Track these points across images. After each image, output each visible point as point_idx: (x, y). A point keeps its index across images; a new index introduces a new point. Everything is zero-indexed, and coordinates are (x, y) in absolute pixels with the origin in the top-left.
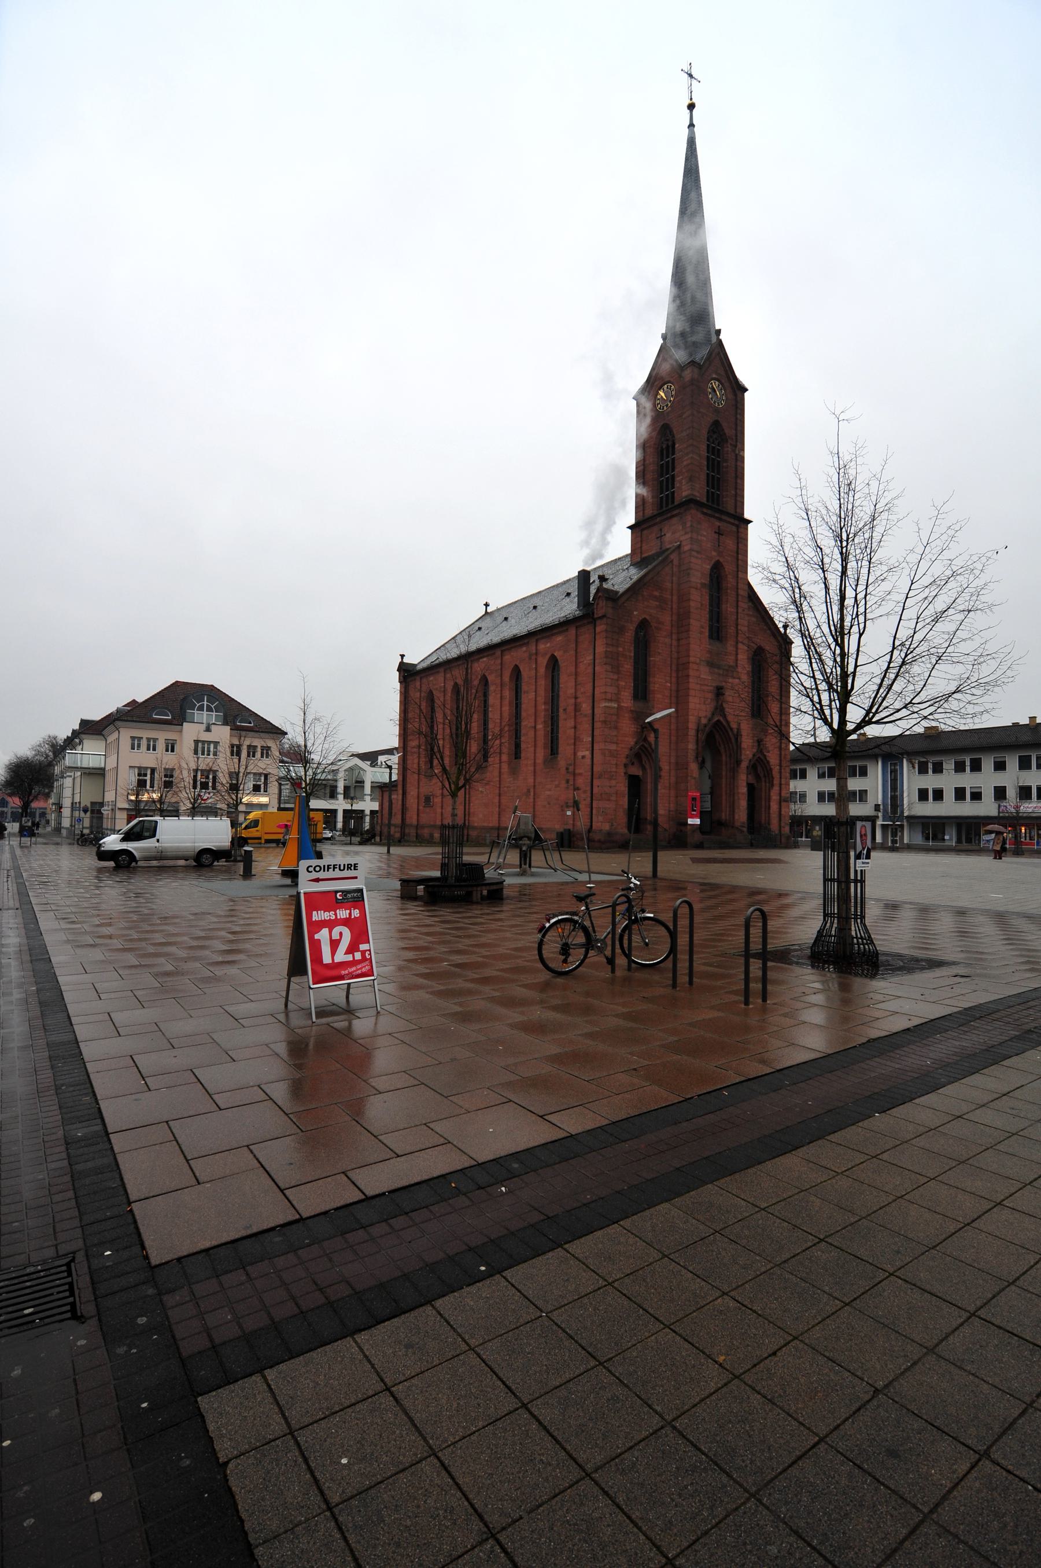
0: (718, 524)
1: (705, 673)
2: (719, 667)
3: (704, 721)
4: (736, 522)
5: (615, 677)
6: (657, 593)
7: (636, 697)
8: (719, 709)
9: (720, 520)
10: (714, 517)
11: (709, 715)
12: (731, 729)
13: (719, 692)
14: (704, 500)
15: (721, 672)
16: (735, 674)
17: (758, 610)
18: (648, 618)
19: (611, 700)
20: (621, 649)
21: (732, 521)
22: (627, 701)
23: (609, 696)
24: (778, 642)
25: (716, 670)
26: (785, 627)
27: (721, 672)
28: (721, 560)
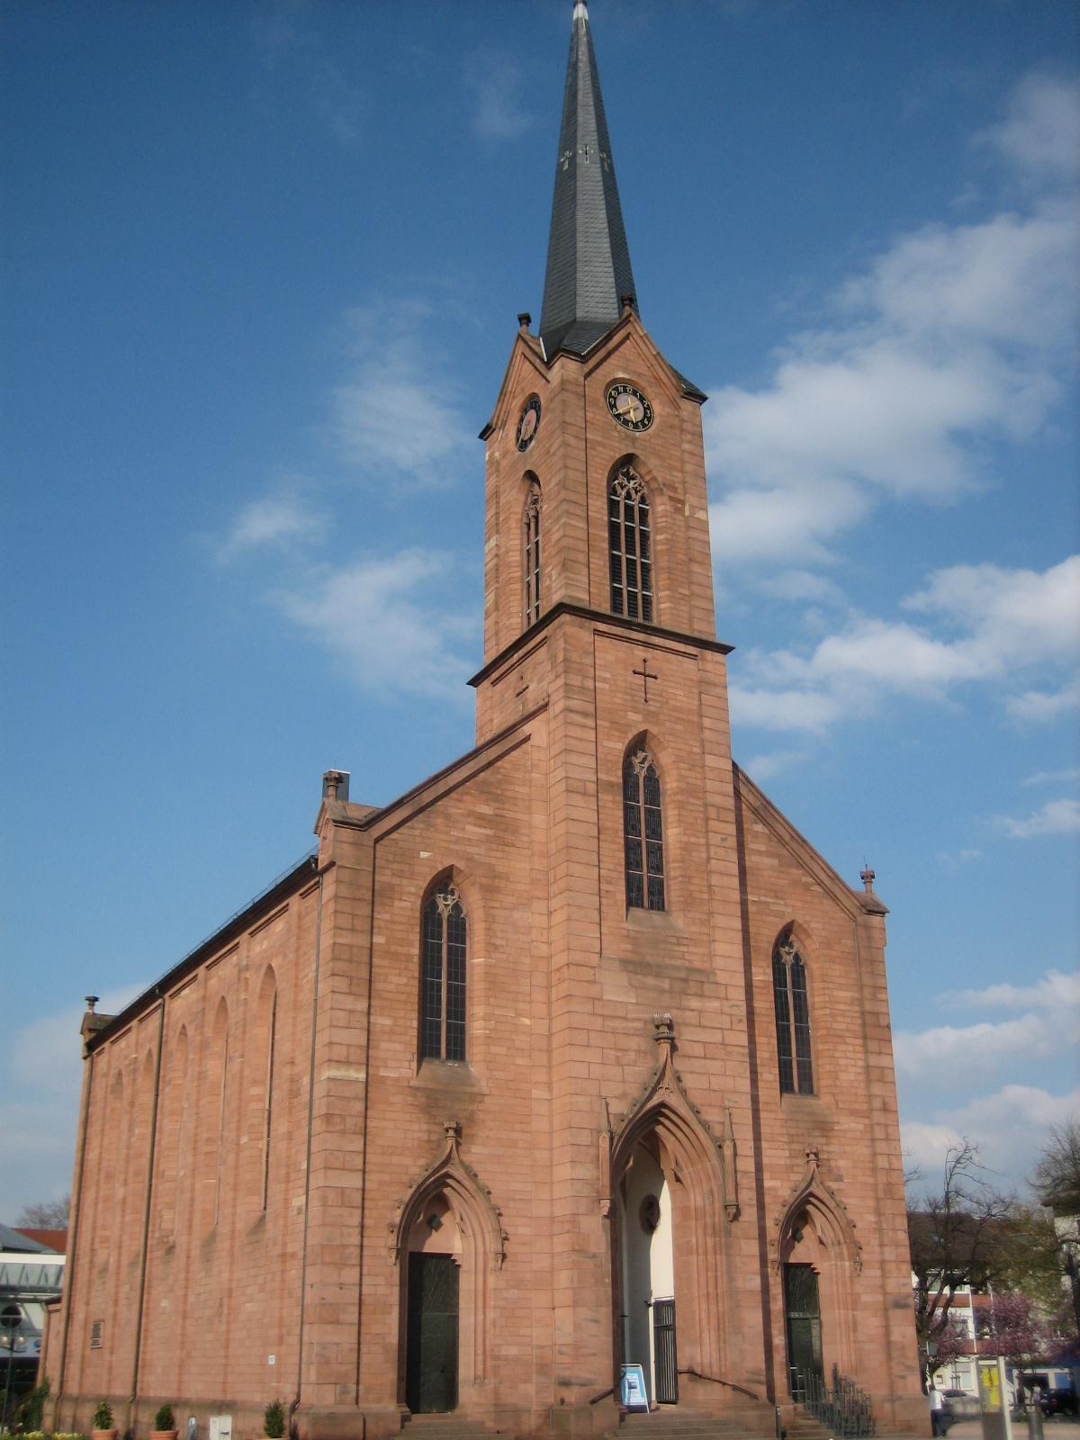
0: (640, 652)
3: (619, 1107)
6: (486, 810)
7: (427, 1048)
9: (646, 645)
10: (629, 640)
11: (635, 1091)
12: (706, 1126)
13: (665, 1033)
14: (609, 612)
15: (666, 984)
16: (708, 989)
17: (780, 840)
18: (460, 865)
19: (347, 1063)
22: (398, 1057)
23: (339, 1052)
24: (844, 909)
25: (650, 981)
26: (868, 877)
27: (666, 984)
28: (654, 730)
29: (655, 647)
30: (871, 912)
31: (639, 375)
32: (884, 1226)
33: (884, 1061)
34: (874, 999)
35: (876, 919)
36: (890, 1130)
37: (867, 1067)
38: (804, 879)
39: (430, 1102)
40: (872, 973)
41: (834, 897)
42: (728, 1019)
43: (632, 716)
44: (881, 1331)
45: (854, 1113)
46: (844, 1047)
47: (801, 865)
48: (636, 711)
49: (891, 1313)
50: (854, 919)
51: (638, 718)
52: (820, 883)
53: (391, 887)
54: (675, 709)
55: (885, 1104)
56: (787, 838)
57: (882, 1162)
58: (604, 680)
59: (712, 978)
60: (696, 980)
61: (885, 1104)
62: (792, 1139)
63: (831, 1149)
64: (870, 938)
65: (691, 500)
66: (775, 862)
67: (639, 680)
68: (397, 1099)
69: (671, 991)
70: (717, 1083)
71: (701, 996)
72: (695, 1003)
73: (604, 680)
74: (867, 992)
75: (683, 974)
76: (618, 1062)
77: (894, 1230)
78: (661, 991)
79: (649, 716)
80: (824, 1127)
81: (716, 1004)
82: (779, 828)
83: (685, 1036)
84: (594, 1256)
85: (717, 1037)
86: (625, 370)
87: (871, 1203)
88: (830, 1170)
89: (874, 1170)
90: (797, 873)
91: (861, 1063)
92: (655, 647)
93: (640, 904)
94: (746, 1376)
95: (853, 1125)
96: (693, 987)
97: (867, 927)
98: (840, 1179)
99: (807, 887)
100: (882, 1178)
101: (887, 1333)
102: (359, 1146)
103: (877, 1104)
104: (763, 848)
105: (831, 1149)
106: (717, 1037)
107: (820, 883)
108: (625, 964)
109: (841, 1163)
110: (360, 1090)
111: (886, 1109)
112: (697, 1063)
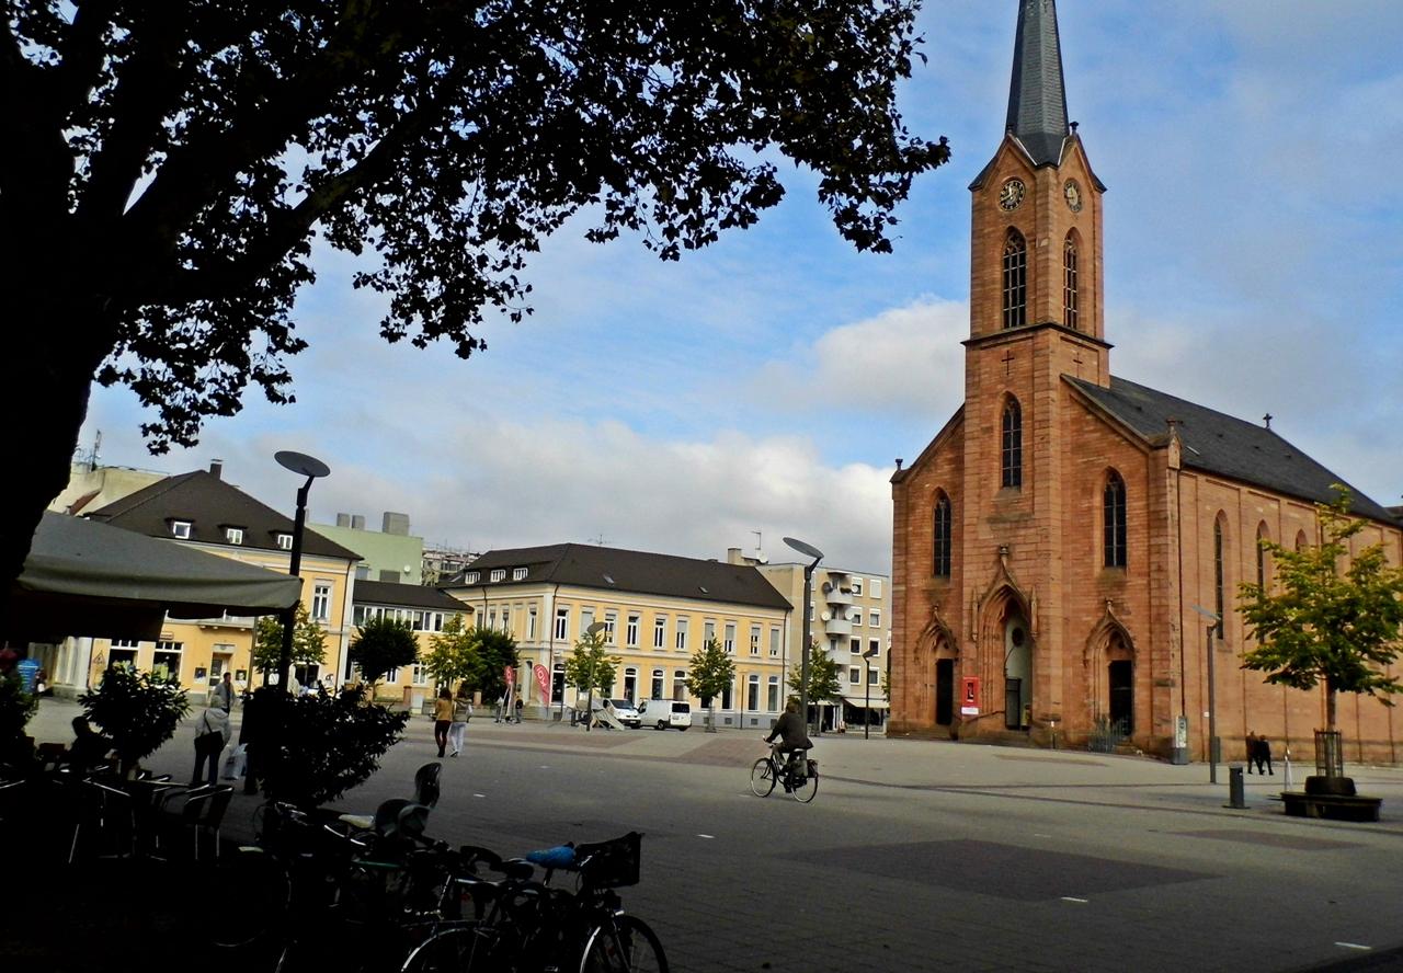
0: (1005, 349)
1: (985, 533)
2: (1004, 522)
3: (983, 590)
4: (1030, 335)
5: (903, 559)
7: (937, 572)
8: (1004, 572)
9: (1007, 343)
11: (990, 581)
17: (1102, 422)
18: (941, 486)
20: (911, 529)
21: (1024, 336)
25: (1001, 526)
27: (1008, 526)
28: (1011, 390)
29: (1012, 342)
30: (1158, 448)
31: (1014, 171)
32: (1153, 639)
33: (1161, 541)
34: (1157, 502)
35: (1162, 452)
36: (1163, 582)
37: (1149, 546)
38: (1118, 439)
39: (929, 595)
40: (1157, 487)
41: (1133, 445)
42: (1039, 538)
43: (999, 387)
44: (1148, 699)
45: (1140, 575)
46: (1137, 536)
47: (1114, 431)
48: (1002, 382)
49: (1154, 689)
50: (1146, 455)
51: (1002, 386)
52: (1126, 439)
53: (914, 504)
54: (1023, 373)
55: (1159, 566)
56: (1104, 418)
57: (1155, 602)
58: (986, 373)
59: (1033, 517)
60: (1024, 520)
61: (1159, 566)
62: (1100, 593)
63: (1124, 597)
64: (1157, 466)
65: (1039, 236)
66: (1098, 435)
67: (1005, 364)
68: (917, 596)
69: (1011, 529)
70: (1032, 571)
71: (1025, 528)
72: (1022, 532)
73: (986, 373)
74: (1152, 500)
75: (1016, 519)
76: (985, 569)
77: (1161, 642)
78: (1006, 530)
79: (1009, 383)
80: (1121, 586)
81: (1032, 531)
82: (1100, 415)
83: (1020, 551)
84: (972, 660)
85: (1033, 547)
86: (1008, 174)
87: (1147, 626)
88: (1123, 609)
89: (1150, 606)
90: (1112, 437)
91: (1146, 544)
92: (1012, 342)
93: (1009, 486)
94: (1039, 716)
95: (1140, 582)
96: (1022, 524)
97: (1155, 459)
98: (1129, 613)
99: (1119, 444)
100: (1154, 611)
101: (1152, 701)
102: (903, 617)
103: (1154, 567)
104: (1092, 428)
105: (1124, 597)
106: (1033, 547)
107: (1126, 439)
108: (992, 521)
109: (1129, 605)
110: (902, 594)
111: (1160, 569)
112: (1023, 564)
